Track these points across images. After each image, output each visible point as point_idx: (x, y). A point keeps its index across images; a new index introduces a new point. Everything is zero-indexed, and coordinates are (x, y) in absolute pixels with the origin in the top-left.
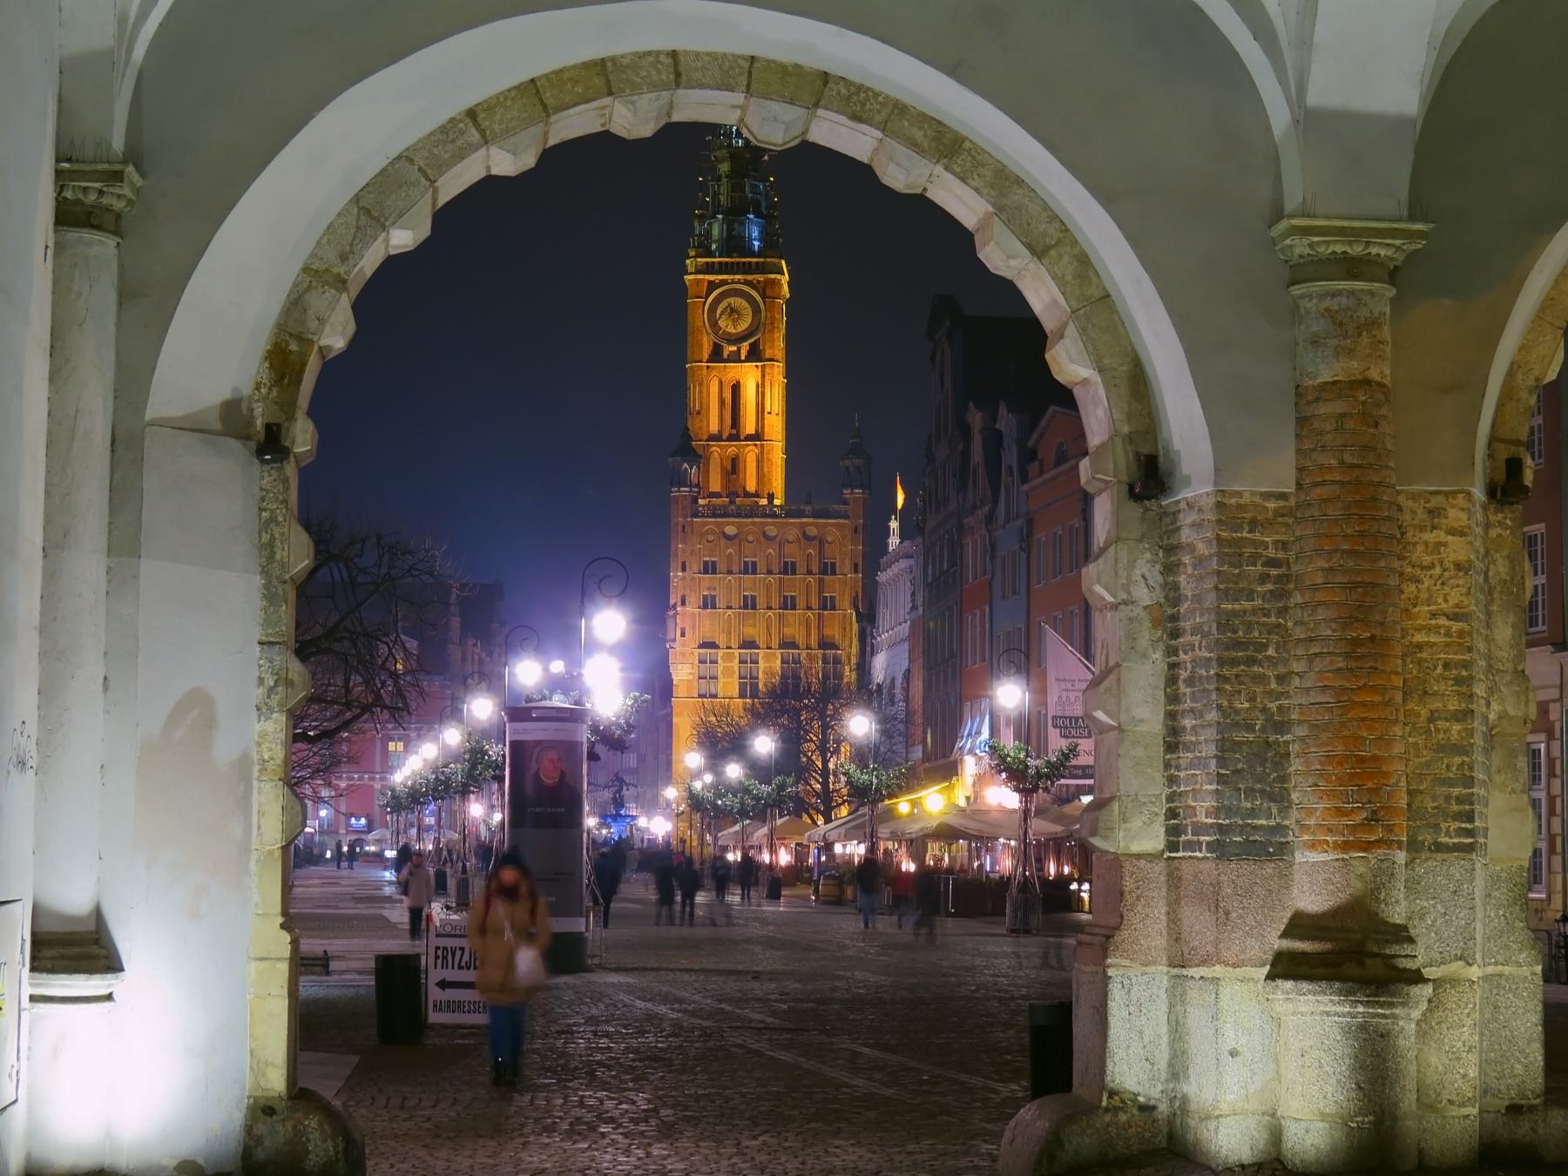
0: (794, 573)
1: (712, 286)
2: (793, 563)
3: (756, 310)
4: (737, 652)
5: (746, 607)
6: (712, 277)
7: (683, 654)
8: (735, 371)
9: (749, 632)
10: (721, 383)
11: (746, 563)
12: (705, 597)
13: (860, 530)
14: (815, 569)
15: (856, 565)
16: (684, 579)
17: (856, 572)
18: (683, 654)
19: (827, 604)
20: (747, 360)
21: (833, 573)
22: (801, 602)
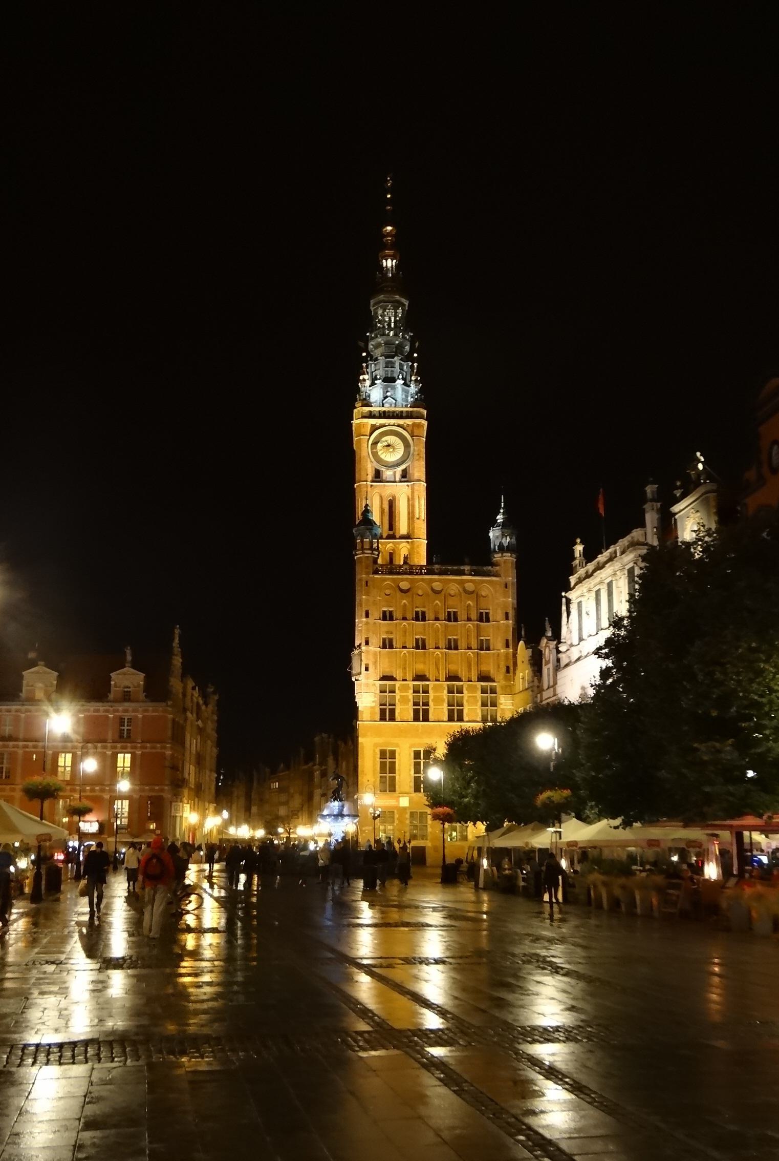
0: (456, 620)
1: (374, 428)
2: (455, 613)
3: (407, 445)
4: (411, 684)
5: (417, 647)
7: (367, 685)
8: (389, 490)
9: (420, 667)
10: (381, 498)
11: (417, 613)
12: (384, 640)
13: (510, 586)
14: (474, 616)
15: (507, 614)
16: (367, 623)
17: (507, 619)
19: (484, 646)
21: (488, 620)
22: (462, 644)
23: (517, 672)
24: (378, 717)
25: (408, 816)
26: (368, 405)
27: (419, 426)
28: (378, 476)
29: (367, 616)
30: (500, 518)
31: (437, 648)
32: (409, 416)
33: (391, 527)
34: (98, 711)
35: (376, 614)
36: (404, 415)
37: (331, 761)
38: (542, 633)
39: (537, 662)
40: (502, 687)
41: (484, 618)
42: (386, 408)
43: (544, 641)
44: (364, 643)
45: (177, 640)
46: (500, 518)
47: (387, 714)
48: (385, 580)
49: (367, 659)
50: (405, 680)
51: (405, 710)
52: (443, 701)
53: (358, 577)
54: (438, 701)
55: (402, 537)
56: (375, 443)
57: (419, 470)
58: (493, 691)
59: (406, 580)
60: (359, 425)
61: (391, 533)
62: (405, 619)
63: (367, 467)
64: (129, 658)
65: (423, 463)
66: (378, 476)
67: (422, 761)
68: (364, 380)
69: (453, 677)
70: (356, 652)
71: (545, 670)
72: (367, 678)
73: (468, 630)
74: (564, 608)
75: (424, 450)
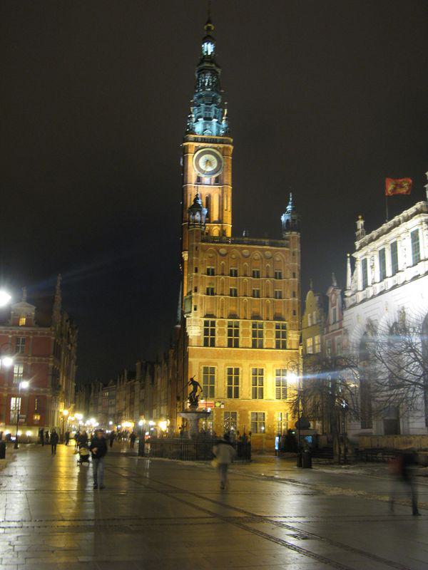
0: (258, 277)
1: (198, 149)
3: (219, 161)
5: (231, 295)
6: (197, 144)
7: (195, 320)
9: (234, 309)
11: (231, 271)
12: (208, 289)
13: (297, 254)
14: (271, 274)
16: (196, 277)
17: (294, 277)
18: (195, 320)
19: (278, 295)
20: (214, 185)
21: (280, 278)
22: (263, 293)
23: (305, 313)
24: (202, 344)
25: (223, 415)
26: (194, 133)
27: (228, 149)
28: (199, 180)
29: (196, 271)
30: (289, 208)
31: (245, 296)
32: (222, 142)
35: (202, 270)
37: (148, 376)
38: (331, 284)
39: (324, 304)
40: (290, 325)
41: (278, 276)
43: (331, 290)
44: (193, 291)
46: (289, 208)
47: (209, 341)
49: (196, 301)
50: (223, 318)
51: (222, 338)
52: (249, 333)
53: (191, 244)
54: (245, 333)
55: (215, 222)
57: (228, 179)
58: (284, 327)
59: (224, 247)
62: (223, 274)
65: (230, 173)
66: (199, 180)
67: (233, 376)
69: (256, 317)
71: (331, 311)
72: (196, 316)
73: (268, 284)
74: (349, 265)
75: (230, 165)
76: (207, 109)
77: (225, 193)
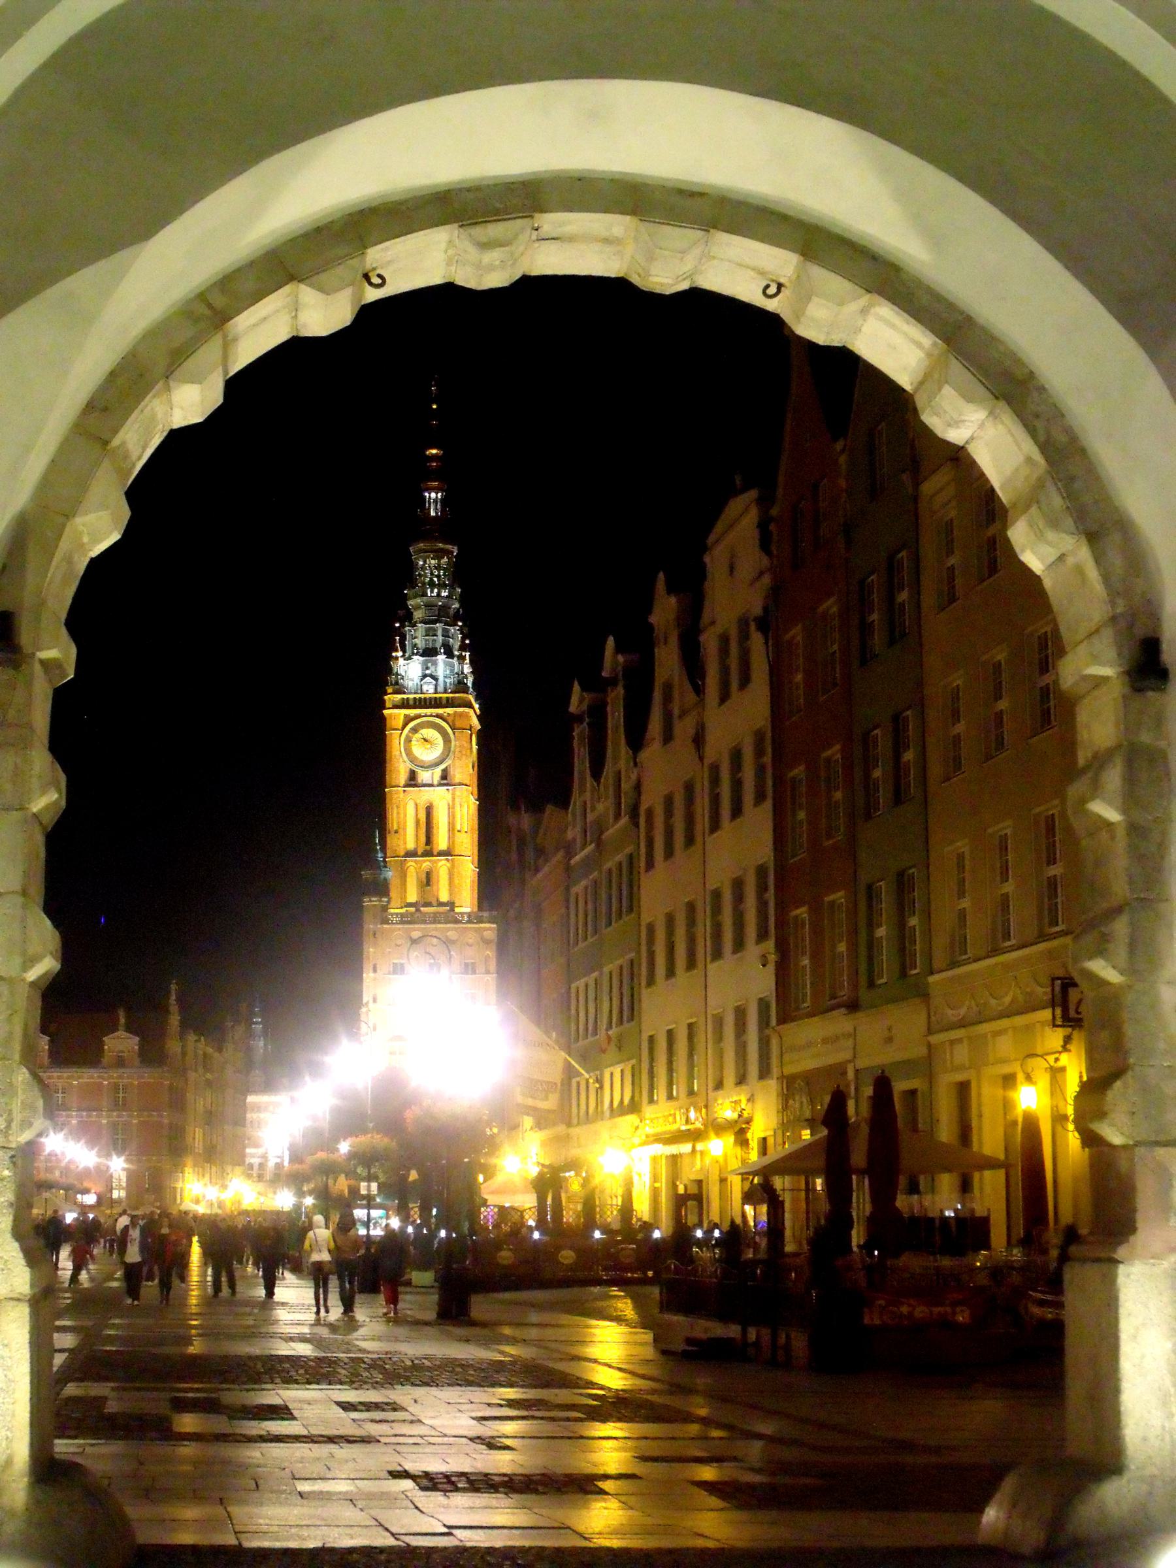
3: (447, 741)
16: (375, 979)
20: (440, 785)
28: (412, 780)
29: (375, 970)
32: (450, 703)
33: (429, 840)
34: (92, 1078)
36: (444, 702)
42: (429, 688)
45: (174, 997)
48: (395, 930)
53: (366, 927)
55: (441, 854)
56: (408, 740)
60: (390, 715)
61: (428, 848)
63: (399, 769)
64: (122, 1021)
66: (412, 776)
68: (397, 658)
70: (364, 1010)
76: (431, 633)
77: (457, 800)
